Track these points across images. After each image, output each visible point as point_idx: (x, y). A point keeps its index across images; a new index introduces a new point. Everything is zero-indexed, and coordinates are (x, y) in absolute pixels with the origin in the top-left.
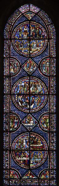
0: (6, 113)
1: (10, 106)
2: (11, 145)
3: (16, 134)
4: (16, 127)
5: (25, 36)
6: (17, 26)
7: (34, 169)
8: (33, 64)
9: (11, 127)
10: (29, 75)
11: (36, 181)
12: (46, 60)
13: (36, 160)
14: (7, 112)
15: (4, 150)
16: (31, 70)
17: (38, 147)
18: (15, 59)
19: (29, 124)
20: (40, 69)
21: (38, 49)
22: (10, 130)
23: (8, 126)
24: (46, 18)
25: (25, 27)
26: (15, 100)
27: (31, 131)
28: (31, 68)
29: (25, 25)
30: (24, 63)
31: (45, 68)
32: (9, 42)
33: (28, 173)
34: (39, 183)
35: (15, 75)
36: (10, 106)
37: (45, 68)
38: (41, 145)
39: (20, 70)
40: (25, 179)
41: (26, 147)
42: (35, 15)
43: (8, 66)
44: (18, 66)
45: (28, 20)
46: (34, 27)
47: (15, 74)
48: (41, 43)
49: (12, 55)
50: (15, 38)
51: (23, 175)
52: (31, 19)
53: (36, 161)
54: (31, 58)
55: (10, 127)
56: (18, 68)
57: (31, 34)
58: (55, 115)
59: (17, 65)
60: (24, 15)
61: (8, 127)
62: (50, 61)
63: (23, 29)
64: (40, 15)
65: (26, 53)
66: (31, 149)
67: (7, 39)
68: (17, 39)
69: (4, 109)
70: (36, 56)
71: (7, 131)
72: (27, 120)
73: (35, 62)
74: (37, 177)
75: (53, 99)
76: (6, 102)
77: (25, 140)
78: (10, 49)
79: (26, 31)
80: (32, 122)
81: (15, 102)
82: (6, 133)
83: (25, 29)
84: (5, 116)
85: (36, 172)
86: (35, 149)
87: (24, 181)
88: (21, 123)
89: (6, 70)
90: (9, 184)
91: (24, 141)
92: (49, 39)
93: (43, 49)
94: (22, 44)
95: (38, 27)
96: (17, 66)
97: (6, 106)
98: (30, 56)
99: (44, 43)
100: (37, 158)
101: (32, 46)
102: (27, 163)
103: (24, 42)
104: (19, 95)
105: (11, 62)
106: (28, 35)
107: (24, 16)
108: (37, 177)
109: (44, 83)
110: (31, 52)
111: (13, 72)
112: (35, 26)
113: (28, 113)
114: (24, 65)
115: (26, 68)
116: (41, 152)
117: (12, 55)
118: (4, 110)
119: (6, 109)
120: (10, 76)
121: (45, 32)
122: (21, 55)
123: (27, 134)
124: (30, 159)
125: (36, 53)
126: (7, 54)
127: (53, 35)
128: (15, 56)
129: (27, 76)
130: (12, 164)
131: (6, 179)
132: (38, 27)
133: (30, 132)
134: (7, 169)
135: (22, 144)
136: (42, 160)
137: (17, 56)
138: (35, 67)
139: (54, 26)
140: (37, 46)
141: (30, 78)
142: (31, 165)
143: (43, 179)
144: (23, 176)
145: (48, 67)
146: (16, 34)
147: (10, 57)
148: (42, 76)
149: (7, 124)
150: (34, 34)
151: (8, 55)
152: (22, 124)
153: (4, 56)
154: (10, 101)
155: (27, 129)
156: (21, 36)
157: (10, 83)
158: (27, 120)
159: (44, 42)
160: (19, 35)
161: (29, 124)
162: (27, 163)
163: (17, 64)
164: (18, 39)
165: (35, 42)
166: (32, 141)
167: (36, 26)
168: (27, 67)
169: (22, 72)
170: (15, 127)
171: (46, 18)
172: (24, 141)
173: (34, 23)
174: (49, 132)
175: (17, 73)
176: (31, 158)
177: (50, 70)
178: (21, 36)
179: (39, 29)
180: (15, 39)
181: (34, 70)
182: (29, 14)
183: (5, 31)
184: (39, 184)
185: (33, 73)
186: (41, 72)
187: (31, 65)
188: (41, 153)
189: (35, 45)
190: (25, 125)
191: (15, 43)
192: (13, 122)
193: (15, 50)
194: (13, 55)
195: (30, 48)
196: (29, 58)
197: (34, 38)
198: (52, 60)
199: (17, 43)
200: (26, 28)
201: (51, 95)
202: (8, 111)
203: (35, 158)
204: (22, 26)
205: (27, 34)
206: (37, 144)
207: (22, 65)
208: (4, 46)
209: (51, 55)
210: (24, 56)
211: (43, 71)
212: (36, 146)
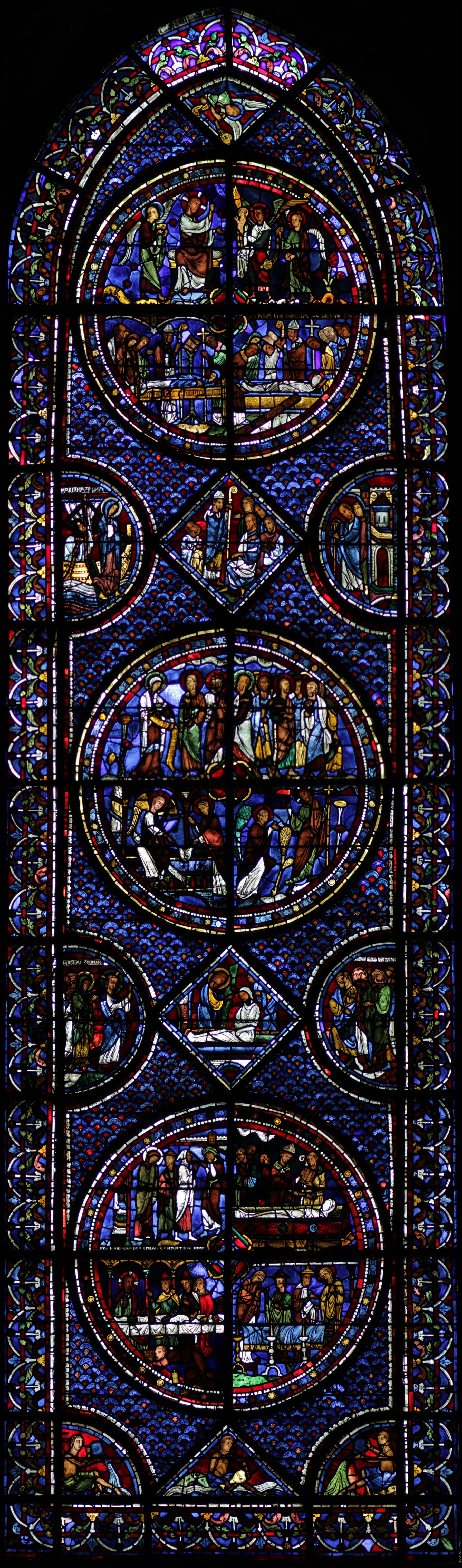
0: (25, 938)
1: (61, 884)
2: (74, 1215)
3: (115, 1114)
4: (113, 1054)
5: (191, 284)
6: (120, 192)
7: (264, 1415)
8: (259, 521)
9: (72, 1056)
10: (220, 617)
11: (286, 1512)
12: (365, 487)
13: (286, 1335)
14: (36, 930)
15: (11, 1257)
16: (243, 569)
17: (301, 1228)
18: (105, 474)
19: (225, 1036)
20: (315, 567)
21: (296, 396)
22: (60, 1081)
23: (48, 1050)
24: (367, 134)
25: (194, 206)
26: (107, 826)
27: (244, 1091)
28: (245, 556)
29: (189, 190)
30: (183, 510)
31: (356, 555)
32: (49, 334)
33: (218, 1447)
34: (307, 1530)
35: (108, 616)
36: (61, 884)
37: (356, 555)
38: (328, 1205)
39: (145, 572)
40: (185, 1498)
41: (197, 1225)
42: (276, 106)
43: (41, 534)
44: (133, 540)
45: (216, 148)
46: (261, 203)
47: (101, 603)
48: (324, 344)
49: (76, 446)
50: (100, 296)
51: (171, 1468)
52: (243, 137)
53: (279, 1342)
54: (243, 470)
55: (66, 1063)
56: (132, 558)
57: (241, 269)
58: (444, 955)
59: (120, 530)
60: (180, 105)
61: (48, 1060)
62: (398, 494)
63: (174, 223)
64: (313, 104)
65: (201, 429)
66: (245, 1241)
67: (37, 311)
68: (119, 308)
69: (15, 903)
70: (281, 456)
71: (37, 1095)
72: (208, 994)
73: (276, 507)
74: (292, 1478)
75: (425, 824)
76: (26, 846)
77: (194, 1164)
78: (62, 390)
79: (194, 245)
80: (251, 1012)
81: (103, 849)
82: (24, 1111)
83: (187, 224)
84: (23, 961)
85: (281, 1436)
86: (275, 1242)
87: (186, 1513)
88: (154, 1026)
89: (23, 570)
90: (57, 1543)
91: (184, 1174)
92: (389, 311)
93: (342, 390)
94: (168, 349)
95: (295, 210)
96: (125, 540)
97: (27, 880)
98: (231, 452)
99: (350, 348)
100: (294, 1324)
101: (244, 367)
102: (207, 1362)
103: (177, 333)
104: (140, 784)
105: (70, 507)
106: (212, 277)
107: (181, 114)
108: (297, 1486)
109: (352, 681)
110: (239, 418)
111: (90, 592)
112: (277, 204)
113: (219, 943)
114: (183, 531)
115: (192, 556)
116: (323, 1272)
117: (76, 446)
118: (13, 912)
119: (25, 910)
120: (61, 622)
121: (353, 249)
122: (153, 447)
123: (210, 1113)
124: (235, 1325)
125: (281, 428)
126: (38, 438)
127: (422, 276)
128: (103, 451)
129: (205, 626)
130: (84, 1371)
131: (22, 1499)
132: (295, 210)
133: (234, 1096)
134: (35, 1415)
135: (167, 1199)
136: (331, 1338)
137: (119, 452)
138: (269, 546)
139: (433, 203)
140: (293, 368)
141: (230, 641)
142: (241, 1380)
143: (343, 1498)
144: (170, 1472)
145: (383, 542)
146: (109, 259)
147: (62, 464)
148: (337, 623)
149: (39, 1035)
150: (268, 264)
151: (44, 446)
152: (164, 1033)
153: (13, 454)
154: (62, 838)
155: (204, 1075)
156: (156, 282)
157: (63, 681)
158: (208, 994)
159: (346, 333)
160: (135, 276)
161: (225, 1036)
162: (207, 1362)
163: (123, 520)
164: (132, 309)
165: (274, 336)
166: (247, 1175)
167: (286, 198)
168: (203, 547)
169: (163, 587)
170: (104, 1059)
171: (367, 134)
172: (184, 1174)
173: (264, 174)
174: (395, 1100)
175: (127, 600)
176: (243, 1323)
177: (399, 574)
178: (156, 282)
179: (304, 227)
180: (105, 307)
181: (262, 569)
182: (223, 99)
183: (16, 235)
184: (311, 1540)
185: (265, 591)
186: (326, 590)
187: (239, 528)
188: (324, 1281)
189: (271, 361)
190: (192, 1037)
191: (104, 341)
192: (89, 1018)
193: (105, 403)
194: (92, 449)
195: (230, 387)
196: (223, 468)
197: (262, 296)
198: (413, 489)
199: (118, 346)
200: (196, 217)
201: (410, 782)
202: (47, 921)
203: (272, 1323)
204: (166, 198)
205: (202, 268)
206: (295, 1205)
207: (163, 530)
208: (11, 368)
209: (411, 446)
210: (180, 454)
211: (338, 580)
212: (281, 1214)
